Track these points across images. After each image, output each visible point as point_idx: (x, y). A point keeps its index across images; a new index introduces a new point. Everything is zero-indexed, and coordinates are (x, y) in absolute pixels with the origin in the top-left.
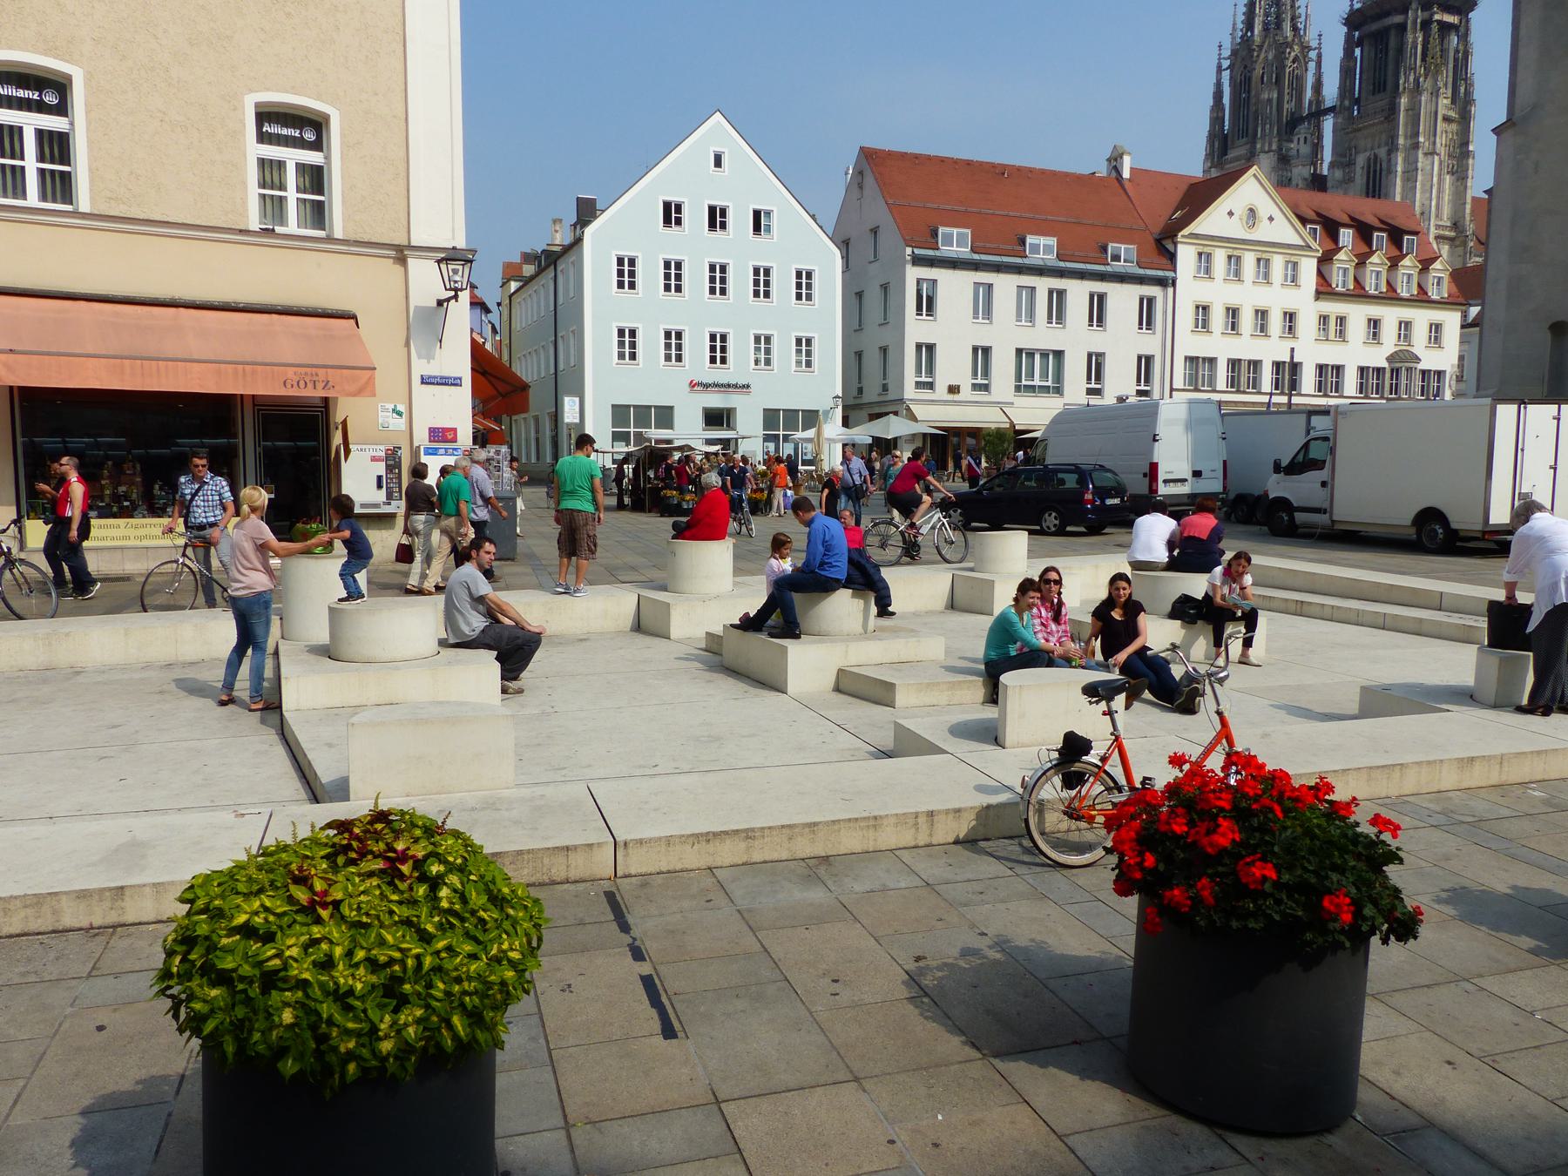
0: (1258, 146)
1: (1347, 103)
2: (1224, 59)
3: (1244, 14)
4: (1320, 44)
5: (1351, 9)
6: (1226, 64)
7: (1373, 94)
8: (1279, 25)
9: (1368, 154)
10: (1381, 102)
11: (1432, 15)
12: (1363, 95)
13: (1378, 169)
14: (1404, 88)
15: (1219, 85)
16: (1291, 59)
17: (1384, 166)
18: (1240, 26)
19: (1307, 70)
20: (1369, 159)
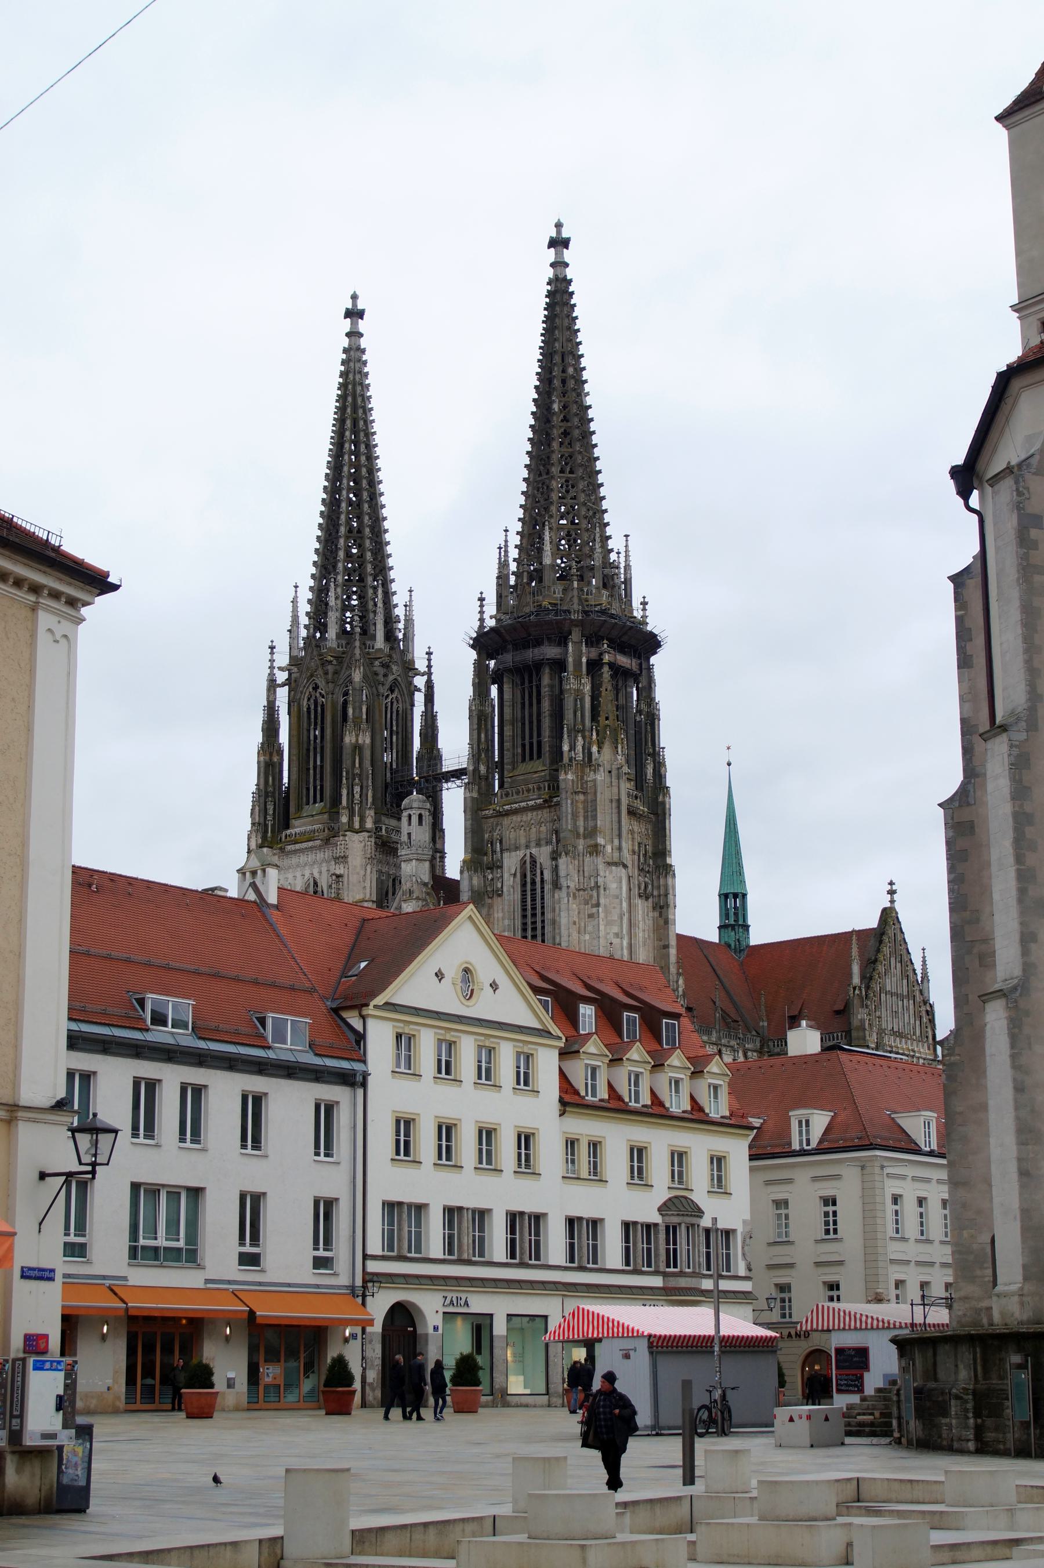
0: (344, 819)
1: (483, 769)
2: (281, 669)
3: (309, 601)
5: (482, 626)
6: (282, 677)
7: (524, 760)
8: (366, 633)
9: (520, 854)
11: (601, 654)
13: (538, 879)
14: (571, 759)
15: (271, 710)
16: (387, 686)
17: (547, 875)
18: (304, 620)
19: (413, 705)
20: (523, 863)
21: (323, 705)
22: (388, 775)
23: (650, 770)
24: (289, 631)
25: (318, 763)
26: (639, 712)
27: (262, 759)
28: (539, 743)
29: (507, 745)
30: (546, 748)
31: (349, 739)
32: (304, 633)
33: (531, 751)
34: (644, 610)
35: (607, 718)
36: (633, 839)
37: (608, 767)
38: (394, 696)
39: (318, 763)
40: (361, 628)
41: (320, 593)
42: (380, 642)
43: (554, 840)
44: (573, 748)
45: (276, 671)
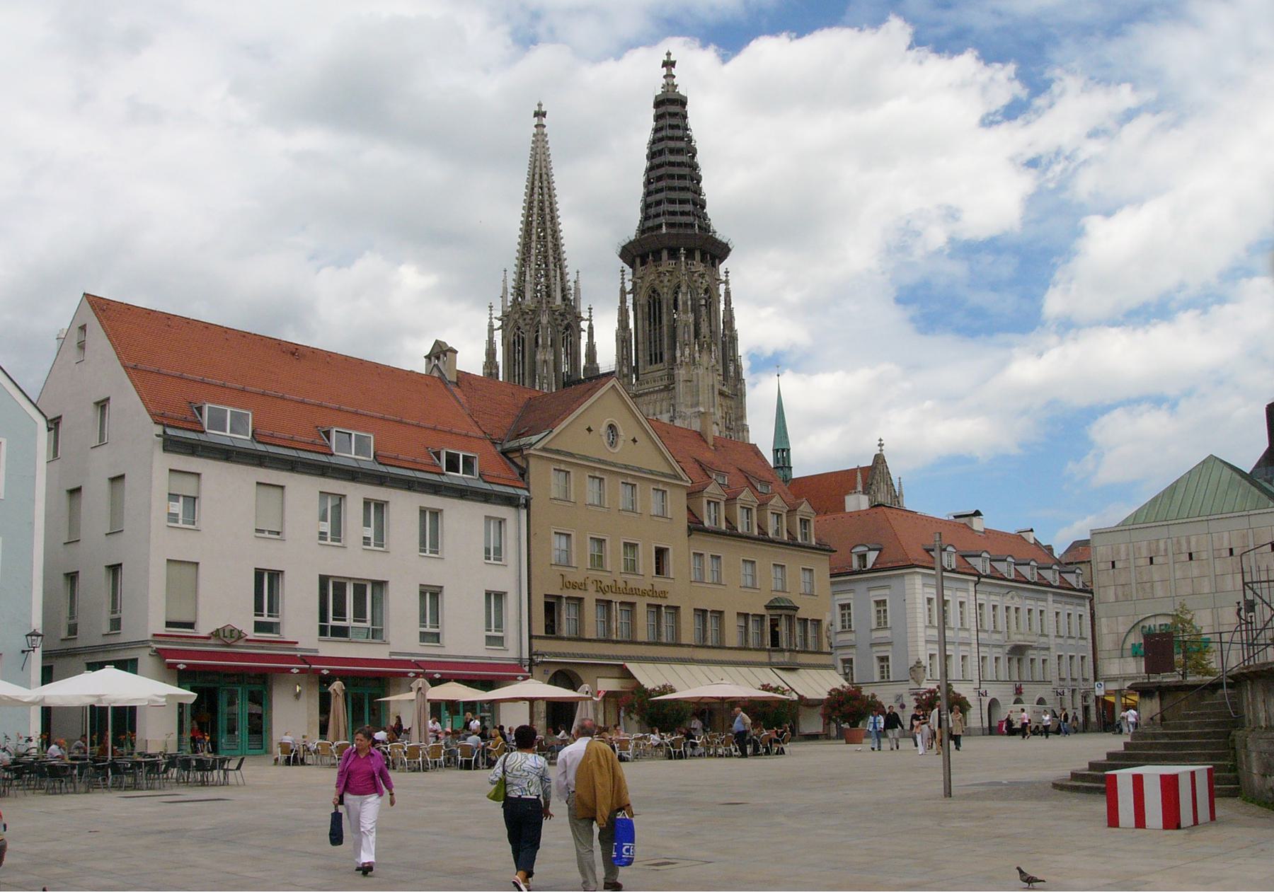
1: (625, 370)
4: (590, 316)
6: (497, 324)
7: (651, 364)
10: (659, 370)
12: (641, 364)
15: (491, 342)
16: (563, 327)
18: (511, 290)
21: (523, 338)
22: (565, 378)
23: (732, 368)
24: (502, 297)
25: (521, 372)
26: (724, 335)
27: (485, 371)
28: (661, 354)
29: (640, 355)
30: (666, 357)
31: (540, 357)
32: (510, 298)
33: (656, 358)
34: (727, 276)
35: (704, 337)
36: (722, 409)
37: (706, 365)
38: (569, 332)
39: (521, 372)
40: (546, 292)
41: (522, 275)
42: (559, 301)
43: (672, 410)
44: (682, 354)
45: (493, 320)
